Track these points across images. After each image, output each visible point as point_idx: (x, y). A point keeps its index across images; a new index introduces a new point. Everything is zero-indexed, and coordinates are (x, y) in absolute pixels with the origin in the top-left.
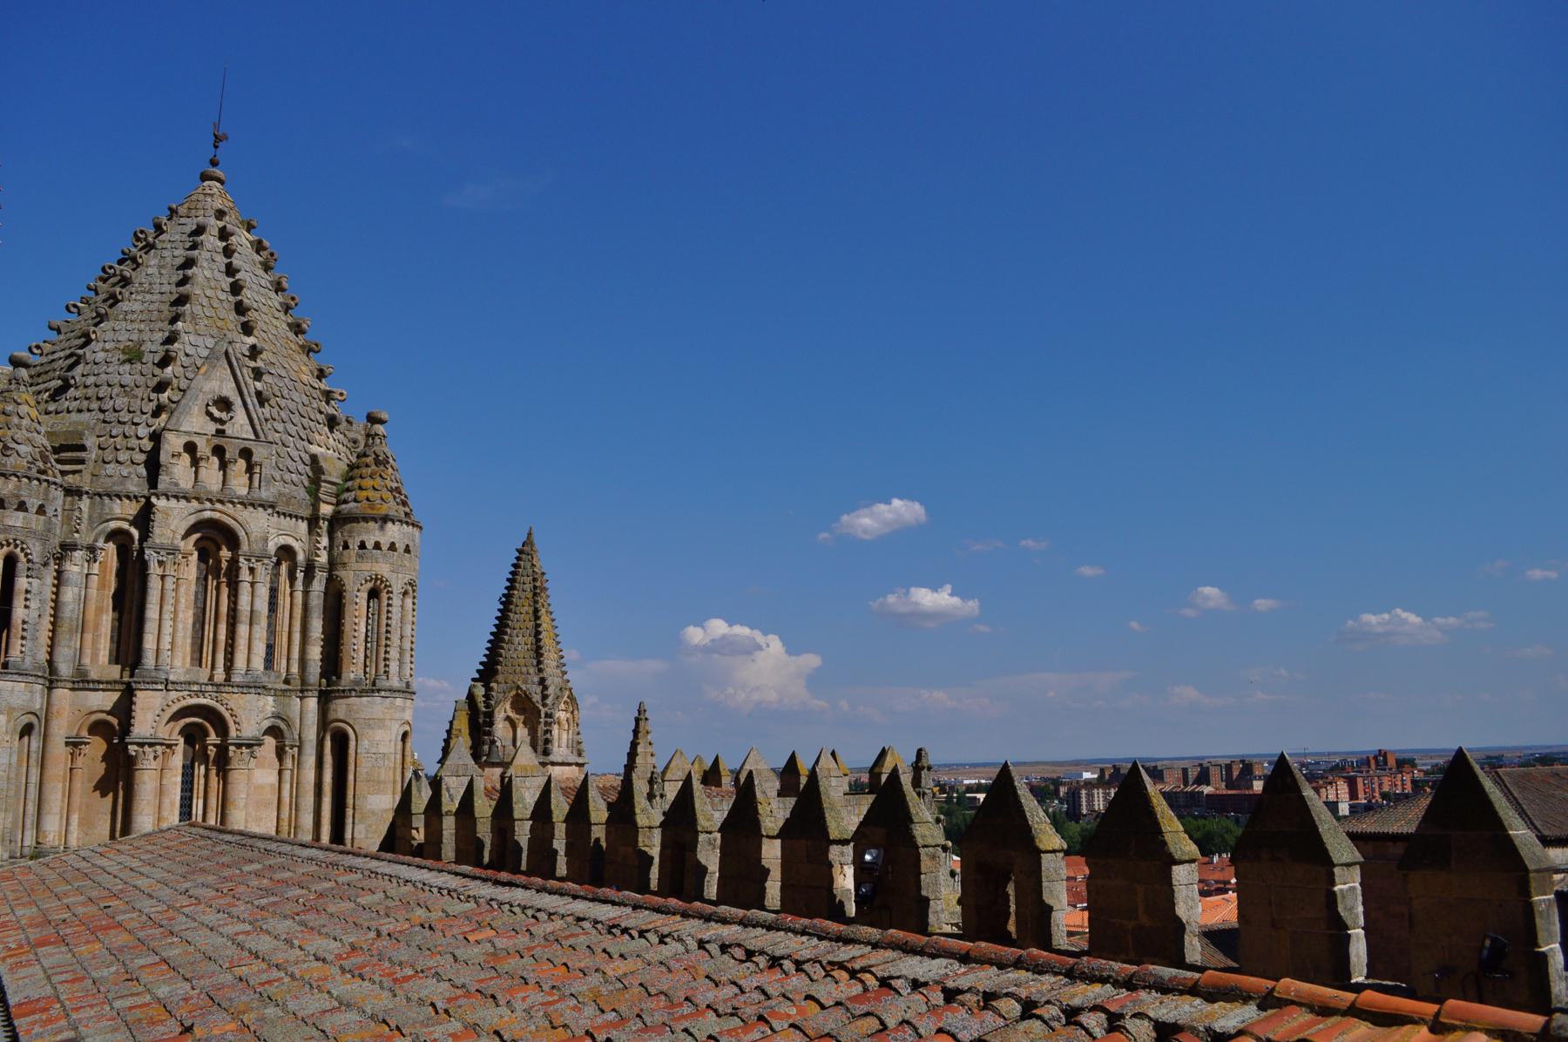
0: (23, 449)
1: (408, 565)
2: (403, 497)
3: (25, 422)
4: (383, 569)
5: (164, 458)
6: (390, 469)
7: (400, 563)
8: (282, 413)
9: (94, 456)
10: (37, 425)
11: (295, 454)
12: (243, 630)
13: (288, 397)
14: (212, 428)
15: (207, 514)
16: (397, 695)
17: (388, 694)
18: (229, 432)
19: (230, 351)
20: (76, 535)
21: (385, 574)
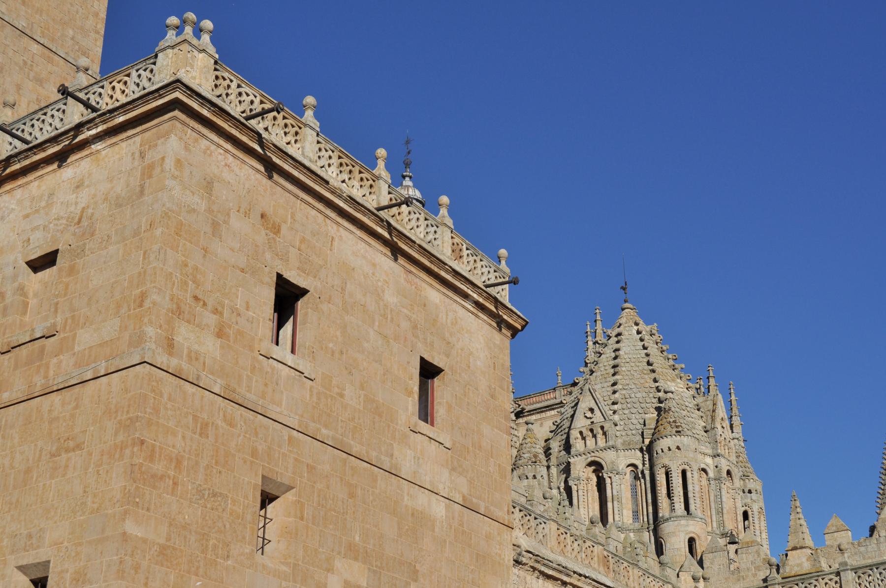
0: (525, 456)
1: (679, 455)
2: (679, 424)
3: (529, 445)
4: (666, 461)
5: (572, 441)
6: (671, 413)
7: (673, 455)
8: (629, 405)
9: (556, 450)
10: (534, 445)
11: (635, 422)
12: (610, 505)
13: (633, 396)
14: (589, 422)
15: (590, 459)
16: (680, 518)
17: (675, 519)
18: (595, 422)
19: (590, 387)
20: (552, 484)
21: (667, 463)
